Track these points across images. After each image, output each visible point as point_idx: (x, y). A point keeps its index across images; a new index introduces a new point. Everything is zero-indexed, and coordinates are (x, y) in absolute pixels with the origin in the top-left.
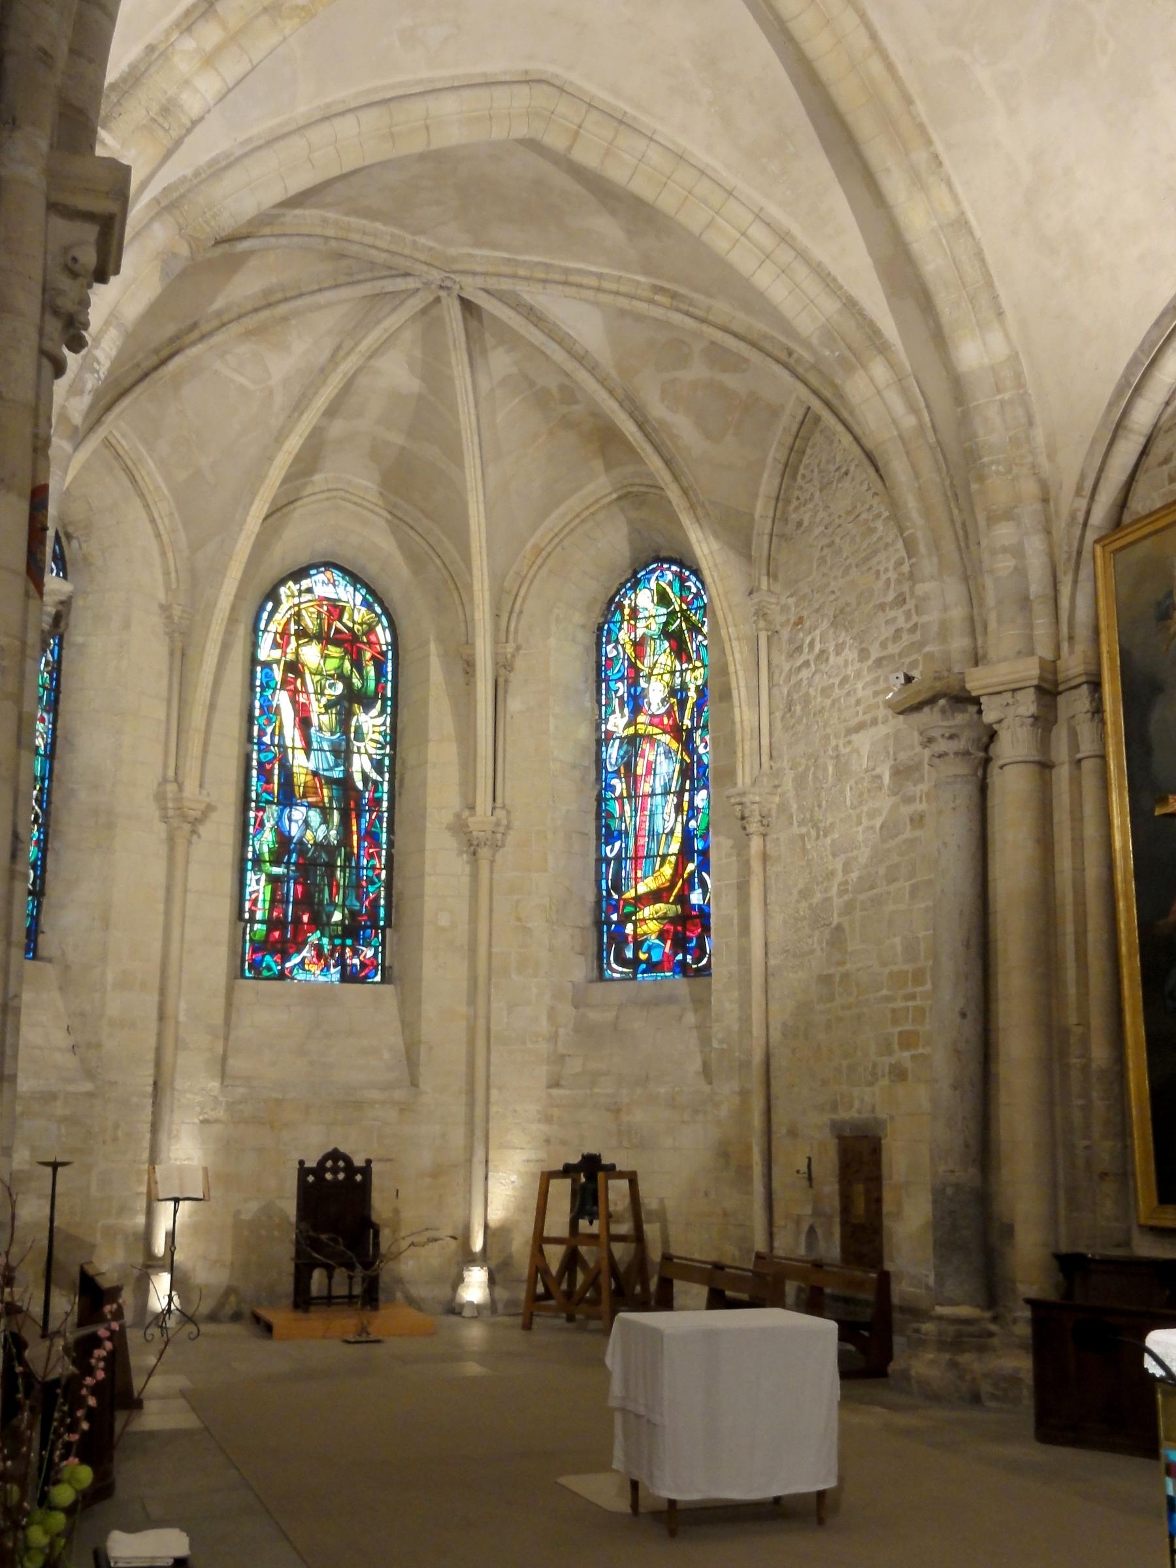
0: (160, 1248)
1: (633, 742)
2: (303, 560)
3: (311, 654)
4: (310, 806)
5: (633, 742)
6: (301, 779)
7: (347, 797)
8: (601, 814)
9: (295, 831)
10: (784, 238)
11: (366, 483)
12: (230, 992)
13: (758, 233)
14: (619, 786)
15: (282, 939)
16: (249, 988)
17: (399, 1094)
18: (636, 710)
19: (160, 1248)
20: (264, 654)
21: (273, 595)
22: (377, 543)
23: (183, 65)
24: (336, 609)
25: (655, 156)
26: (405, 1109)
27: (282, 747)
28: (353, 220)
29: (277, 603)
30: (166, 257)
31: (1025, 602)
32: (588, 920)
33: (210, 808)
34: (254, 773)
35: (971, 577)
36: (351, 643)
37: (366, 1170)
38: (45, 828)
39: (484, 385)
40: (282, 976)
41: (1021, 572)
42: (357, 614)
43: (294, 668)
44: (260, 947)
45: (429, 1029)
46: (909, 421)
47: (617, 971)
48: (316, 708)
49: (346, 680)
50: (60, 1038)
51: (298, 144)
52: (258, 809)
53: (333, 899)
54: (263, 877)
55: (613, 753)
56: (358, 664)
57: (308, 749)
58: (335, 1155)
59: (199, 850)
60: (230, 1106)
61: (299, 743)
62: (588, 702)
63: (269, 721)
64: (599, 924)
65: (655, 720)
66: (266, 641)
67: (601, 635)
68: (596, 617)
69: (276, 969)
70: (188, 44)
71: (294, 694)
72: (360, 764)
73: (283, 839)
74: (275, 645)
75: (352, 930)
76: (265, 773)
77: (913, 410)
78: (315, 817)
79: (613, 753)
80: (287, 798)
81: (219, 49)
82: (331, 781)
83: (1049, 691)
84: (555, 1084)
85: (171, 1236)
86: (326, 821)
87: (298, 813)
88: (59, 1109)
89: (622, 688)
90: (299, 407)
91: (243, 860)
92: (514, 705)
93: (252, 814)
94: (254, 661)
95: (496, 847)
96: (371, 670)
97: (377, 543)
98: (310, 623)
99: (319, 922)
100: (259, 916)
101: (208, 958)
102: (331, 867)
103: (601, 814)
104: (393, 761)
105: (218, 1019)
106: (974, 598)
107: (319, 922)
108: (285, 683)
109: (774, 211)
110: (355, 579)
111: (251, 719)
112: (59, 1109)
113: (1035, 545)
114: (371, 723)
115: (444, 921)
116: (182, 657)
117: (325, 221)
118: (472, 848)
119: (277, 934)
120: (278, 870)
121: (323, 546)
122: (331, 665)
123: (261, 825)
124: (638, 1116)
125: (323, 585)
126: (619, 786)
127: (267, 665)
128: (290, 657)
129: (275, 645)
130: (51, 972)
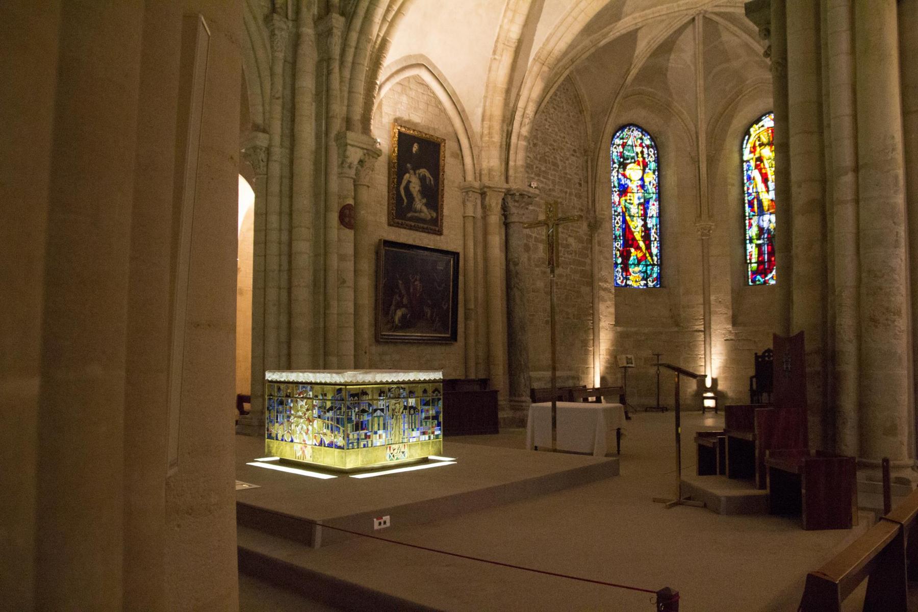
0: (708, 383)
2: (758, 114)
4: (771, 214)
9: (765, 225)
15: (763, 270)
19: (708, 383)
20: (745, 158)
21: (748, 133)
23: (506, 27)
27: (757, 193)
28: (647, 11)
29: (750, 136)
34: (747, 205)
43: (760, 159)
44: (754, 273)
51: (570, 19)
52: (750, 219)
54: (754, 245)
57: (768, 191)
61: (764, 189)
63: (750, 184)
69: (762, 280)
70: (506, 20)
71: (760, 170)
73: (761, 229)
74: (751, 152)
76: (751, 204)
80: (761, 212)
81: (514, 16)
85: (714, 381)
87: (766, 217)
91: (745, 240)
93: (747, 222)
94: (742, 161)
100: (754, 260)
108: (757, 167)
111: (743, 184)
117: (634, 19)
119: (762, 267)
120: (760, 242)
123: (751, 225)
127: (748, 161)
128: (757, 155)
129: (751, 152)
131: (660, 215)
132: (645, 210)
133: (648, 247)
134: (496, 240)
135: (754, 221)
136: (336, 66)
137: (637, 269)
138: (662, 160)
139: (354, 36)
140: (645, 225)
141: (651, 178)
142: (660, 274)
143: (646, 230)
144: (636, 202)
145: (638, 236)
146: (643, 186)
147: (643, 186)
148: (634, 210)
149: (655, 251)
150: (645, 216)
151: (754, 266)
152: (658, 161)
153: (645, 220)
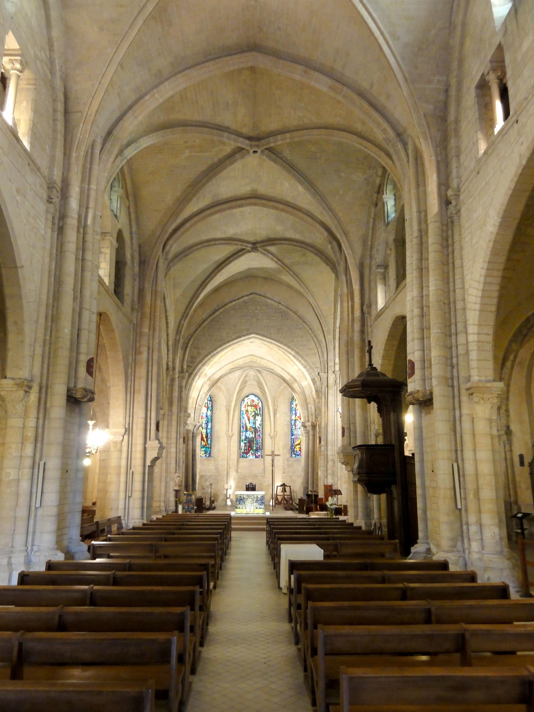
0: (228, 496)
1: (295, 420)
2: (248, 394)
3: (249, 409)
5: (295, 420)
6: (248, 428)
7: (255, 430)
8: (292, 432)
10: (283, 369)
11: (255, 383)
12: (238, 461)
13: (280, 369)
14: (294, 427)
16: (242, 459)
17: (262, 475)
18: (296, 415)
20: (243, 409)
21: (243, 400)
22: (258, 392)
24: (253, 401)
25: (266, 361)
26: (263, 477)
30: (209, 384)
31: (312, 414)
32: (290, 448)
33: (233, 435)
35: (308, 410)
36: (255, 406)
37: (255, 486)
38: (211, 439)
39: (264, 374)
40: (246, 457)
41: (311, 411)
42: (256, 401)
43: (247, 411)
44: (243, 453)
45: (266, 465)
46: (300, 390)
47: (294, 456)
48: (251, 417)
49: (255, 412)
50: (214, 468)
53: (252, 446)
55: (293, 422)
56: (257, 409)
58: (251, 483)
59: (232, 440)
60: (238, 477)
62: (289, 414)
64: (291, 448)
65: (298, 417)
66: (243, 407)
67: (291, 403)
68: (290, 400)
72: (257, 425)
73: (246, 437)
75: (257, 450)
77: (301, 389)
78: (251, 433)
79: (293, 422)
80: (246, 431)
82: (253, 428)
83: (314, 426)
84: (284, 473)
86: (252, 433)
87: (248, 433)
88: (213, 477)
89: (294, 412)
90: (239, 380)
92: (277, 416)
95: (275, 438)
96: (258, 410)
97: (258, 392)
98: (249, 404)
99: (252, 449)
101: (234, 455)
102: (253, 441)
103: (292, 432)
104: (262, 425)
105: (236, 464)
106: (308, 413)
107: (252, 449)
109: (281, 366)
110: (256, 396)
112: (213, 477)
113: (313, 407)
114: (259, 418)
115: (268, 449)
116: (228, 413)
118: (271, 438)
121: (250, 392)
122: (252, 410)
124: (294, 478)
125: (252, 397)
126: (294, 427)
130: (212, 459)
131: (211, 428)
132: (207, 426)
133: (207, 441)
134: (190, 443)
135: (244, 433)
136: (184, 389)
137: (203, 449)
138: (214, 407)
139: (190, 380)
140: (207, 432)
141: (209, 413)
142: (210, 451)
143: (207, 434)
144: (204, 422)
145: (204, 436)
146: (207, 416)
147: (207, 416)
148: (204, 425)
149: (209, 442)
150: (207, 428)
151: (243, 450)
152: (212, 406)
153: (207, 430)
